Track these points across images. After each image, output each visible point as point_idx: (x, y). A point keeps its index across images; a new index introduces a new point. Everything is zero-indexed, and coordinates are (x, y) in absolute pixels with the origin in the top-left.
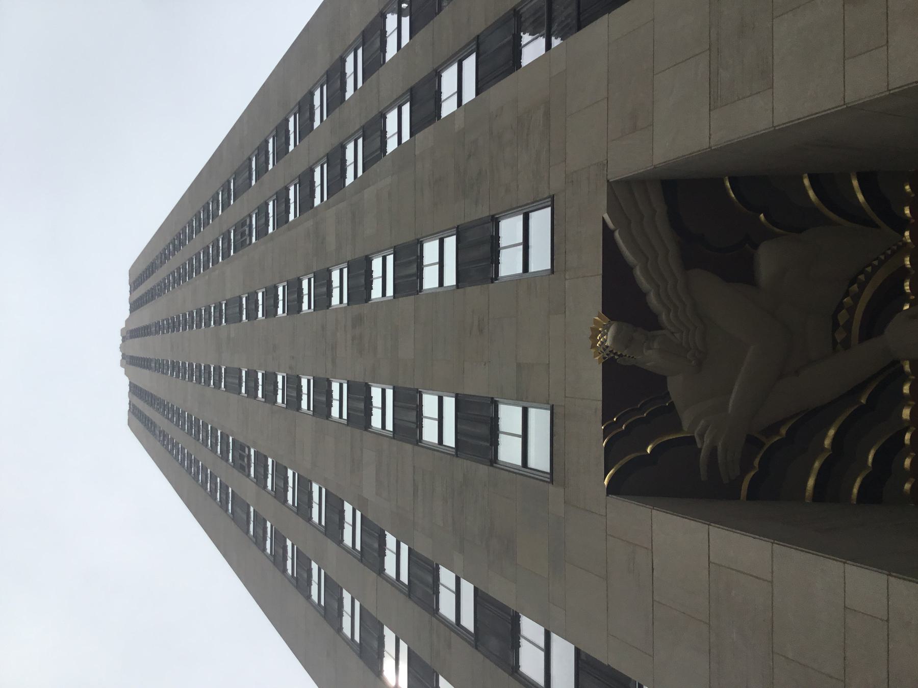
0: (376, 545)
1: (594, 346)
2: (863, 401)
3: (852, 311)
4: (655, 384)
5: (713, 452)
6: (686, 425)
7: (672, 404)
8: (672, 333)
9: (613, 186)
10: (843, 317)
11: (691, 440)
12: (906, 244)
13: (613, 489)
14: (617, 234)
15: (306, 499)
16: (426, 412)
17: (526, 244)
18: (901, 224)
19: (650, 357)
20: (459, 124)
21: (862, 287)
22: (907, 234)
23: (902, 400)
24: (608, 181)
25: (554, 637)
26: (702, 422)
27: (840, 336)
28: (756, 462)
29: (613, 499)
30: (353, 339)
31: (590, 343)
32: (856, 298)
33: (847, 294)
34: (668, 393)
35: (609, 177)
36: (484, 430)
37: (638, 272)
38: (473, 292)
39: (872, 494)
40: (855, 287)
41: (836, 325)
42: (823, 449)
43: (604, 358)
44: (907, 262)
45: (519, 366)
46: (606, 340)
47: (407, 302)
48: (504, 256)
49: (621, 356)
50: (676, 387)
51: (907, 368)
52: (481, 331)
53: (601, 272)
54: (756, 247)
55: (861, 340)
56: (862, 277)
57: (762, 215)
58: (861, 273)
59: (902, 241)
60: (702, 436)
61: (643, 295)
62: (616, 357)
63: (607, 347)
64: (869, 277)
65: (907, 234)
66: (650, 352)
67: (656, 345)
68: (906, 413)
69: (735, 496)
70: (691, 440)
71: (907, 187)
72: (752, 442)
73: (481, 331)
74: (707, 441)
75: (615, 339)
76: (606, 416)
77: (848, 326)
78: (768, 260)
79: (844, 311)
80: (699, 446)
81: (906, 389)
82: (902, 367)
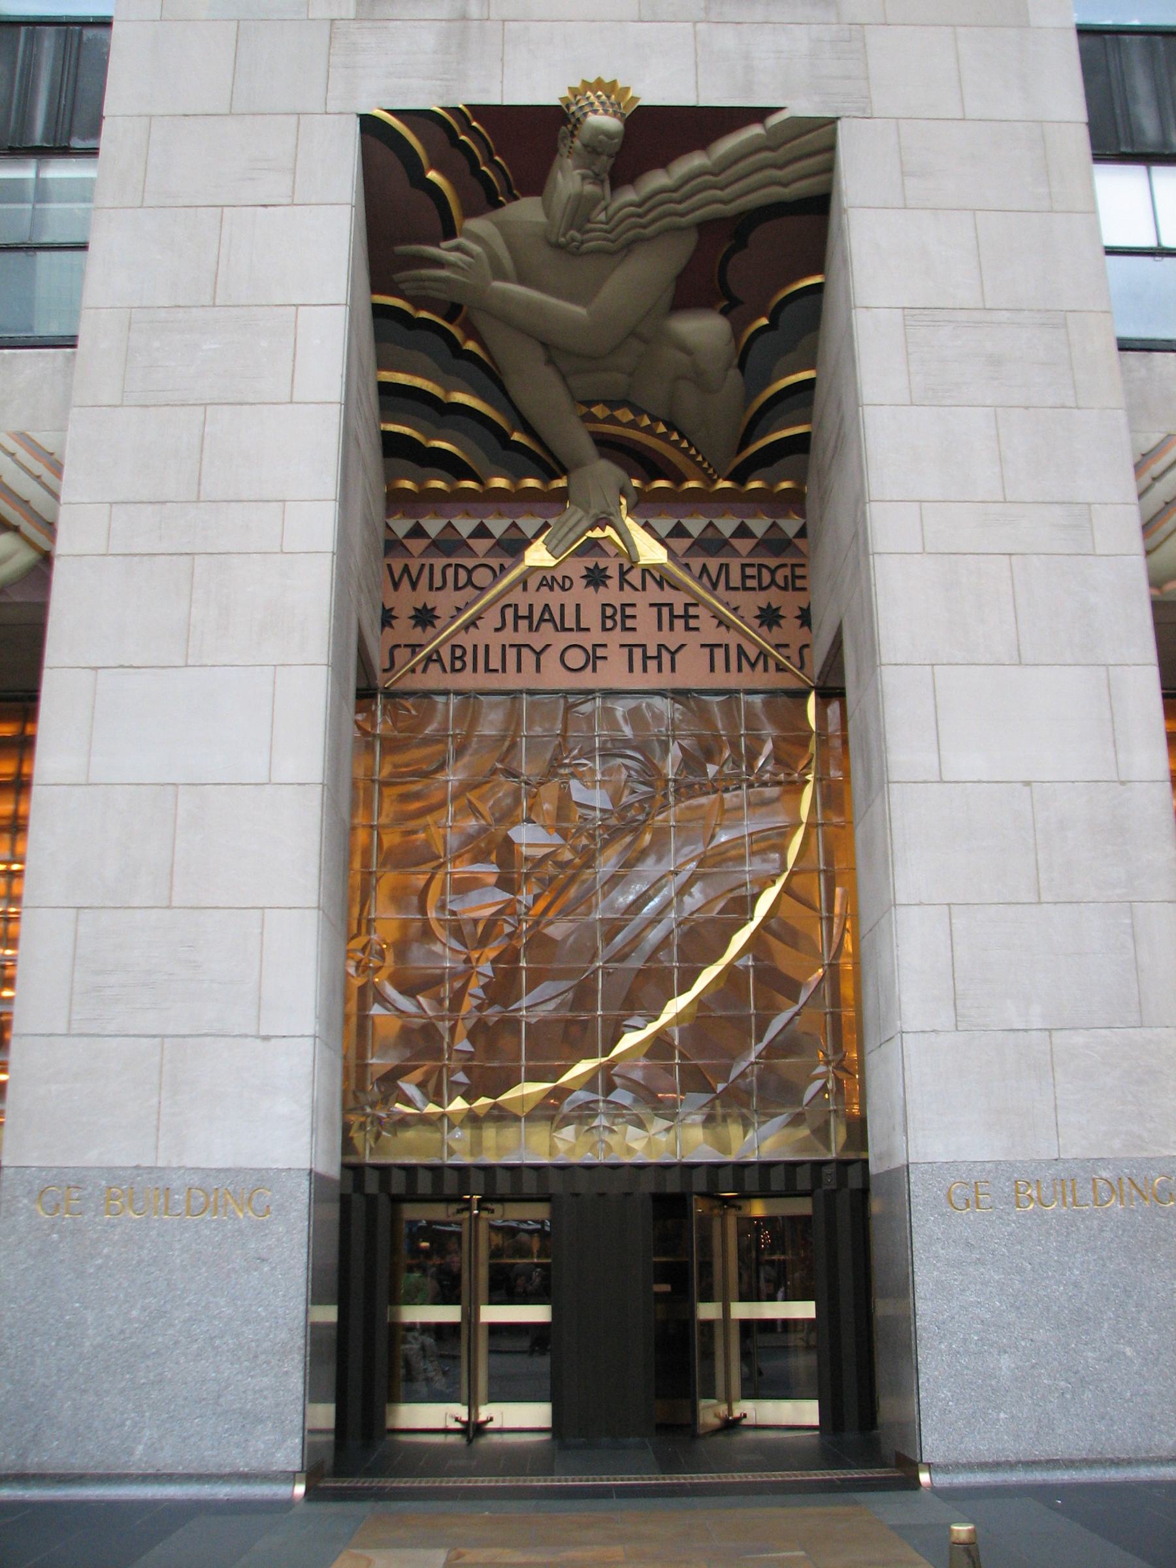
2: (516, 437)
3: (633, 425)
4: (533, 182)
5: (439, 263)
7: (500, 205)
8: (606, 208)
9: (831, 122)
10: (625, 415)
12: (715, 482)
13: (370, 125)
14: (756, 130)
18: (740, 475)
21: (663, 437)
22: (727, 484)
23: (516, 475)
24: (838, 118)
26: (476, 248)
27: (599, 411)
28: (424, 314)
31: (592, 80)
32: (649, 430)
33: (654, 419)
34: (516, 198)
35: (843, 120)
37: (696, 161)
39: (392, 446)
40: (662, 429)
41: (613, 404)
42: (448, 391)
43: (568, 106)
44: (692, 484)
46: (595, 112)
49: (572, 135)
50: (526, 211)
51: (561, 483)
53: (702, 104)
54: (724, 312)
55: (592, 434)
56: (675, 437)
57: (764, 321)
58: (682, 436)
59: (719, 477)
60: (458, 248)
61: (664, 163)
62: (570, 127)
63: (585, 115)
64: (675, 444)
65: (727, 484)
66: (578, 178)
67: (589, 188)
68: (500, 482)
69: (375, 289)
70: (450, 232)
71: (785, 485)
72: (453, 311)
74: (453, 257)
75: (598, 131)
76: (479, 111)
77: (612, 420)
78: (704, 330)
79: (632, 417)
80: (444, 244)
81: (531, 483)
82: (559, 477)
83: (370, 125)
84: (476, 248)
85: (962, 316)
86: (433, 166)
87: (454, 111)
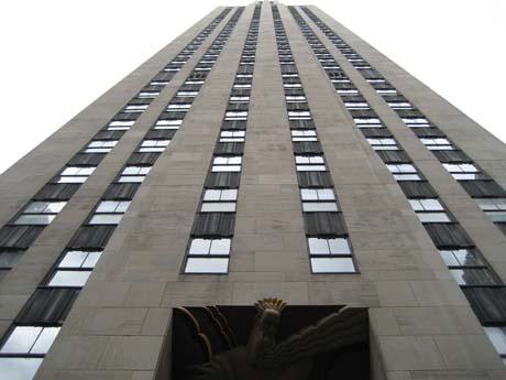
0: (143, 162)
1: (266, 300)
6: (218, 357)
9: (366, 310)
11: (207, 360)
13: (176, 312)
14: (336, 314)
15: (172, 116)
16: (225, 192)
17: (329, 258)
19: (257, 336)
20: (405, 212)
25: (40, 360)
29: (170, 312)
30: (272, 145)
31: (267, 298)
36: (213, 230)
37: (312, 328)
38: (300, 222)
45: (253, 253)
47: (294, 180)
48: (323, 242)
52: (276, 228)
60: (210, 366)
67: (266, 339)
70: (207, 360)
73: (276, 228)
74: (208, 370)
75: (270, 314)
76: (223, 309)
83: (176, 312)
84: (219, 367)
85: (439, 373)
86: (202, 332)
87: (211, 308)
